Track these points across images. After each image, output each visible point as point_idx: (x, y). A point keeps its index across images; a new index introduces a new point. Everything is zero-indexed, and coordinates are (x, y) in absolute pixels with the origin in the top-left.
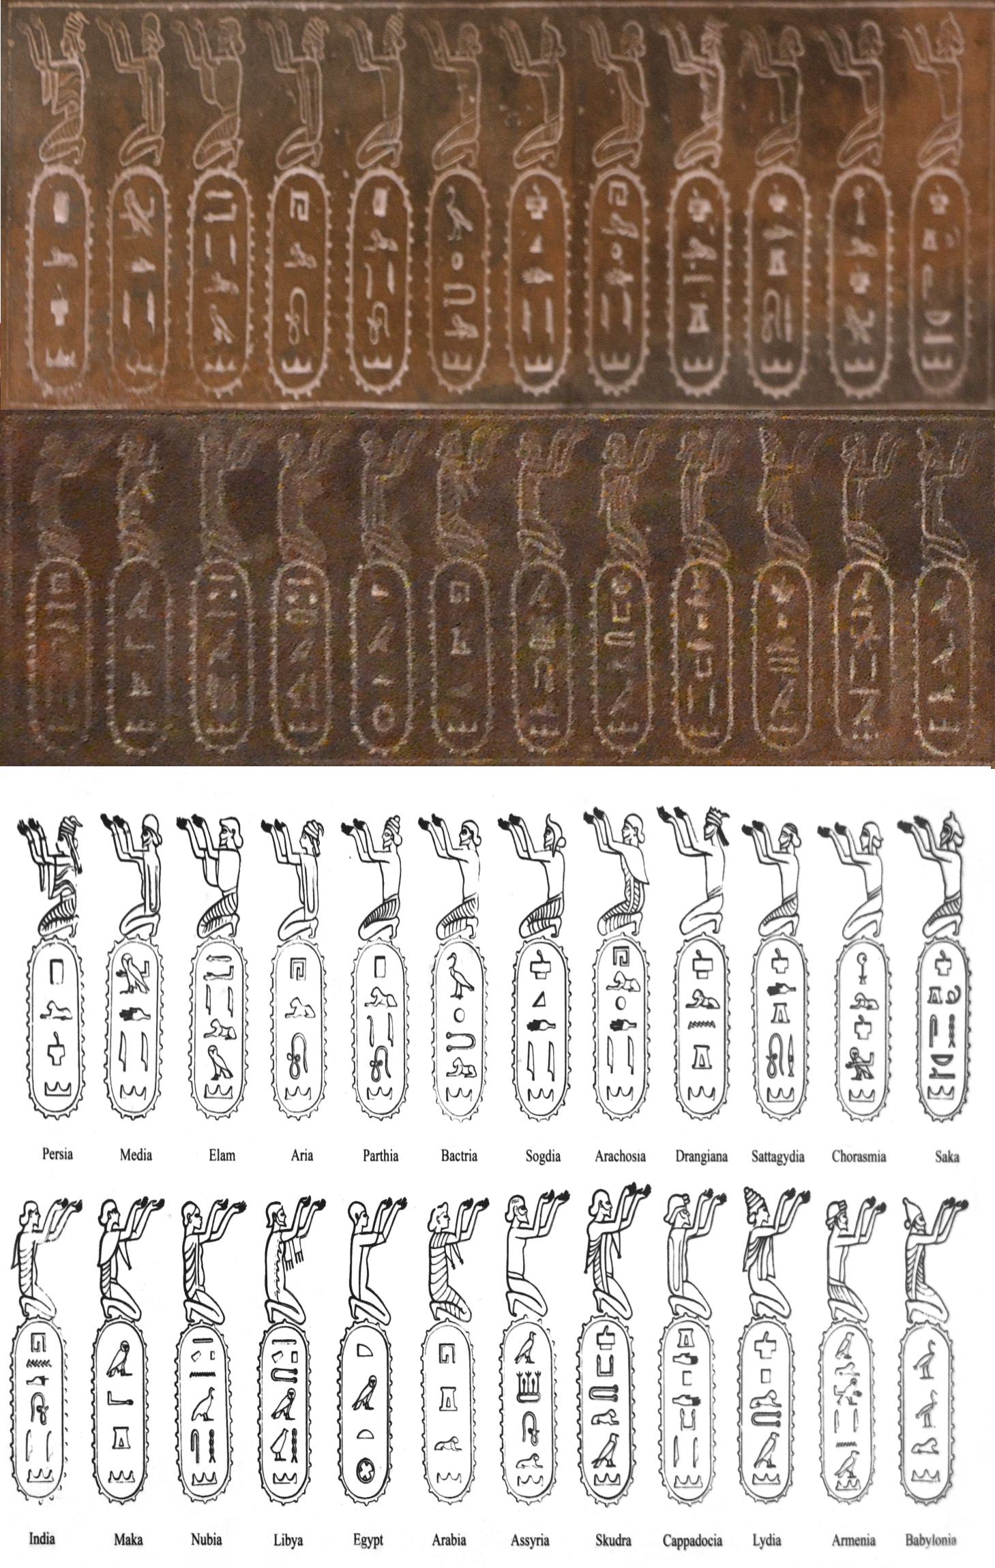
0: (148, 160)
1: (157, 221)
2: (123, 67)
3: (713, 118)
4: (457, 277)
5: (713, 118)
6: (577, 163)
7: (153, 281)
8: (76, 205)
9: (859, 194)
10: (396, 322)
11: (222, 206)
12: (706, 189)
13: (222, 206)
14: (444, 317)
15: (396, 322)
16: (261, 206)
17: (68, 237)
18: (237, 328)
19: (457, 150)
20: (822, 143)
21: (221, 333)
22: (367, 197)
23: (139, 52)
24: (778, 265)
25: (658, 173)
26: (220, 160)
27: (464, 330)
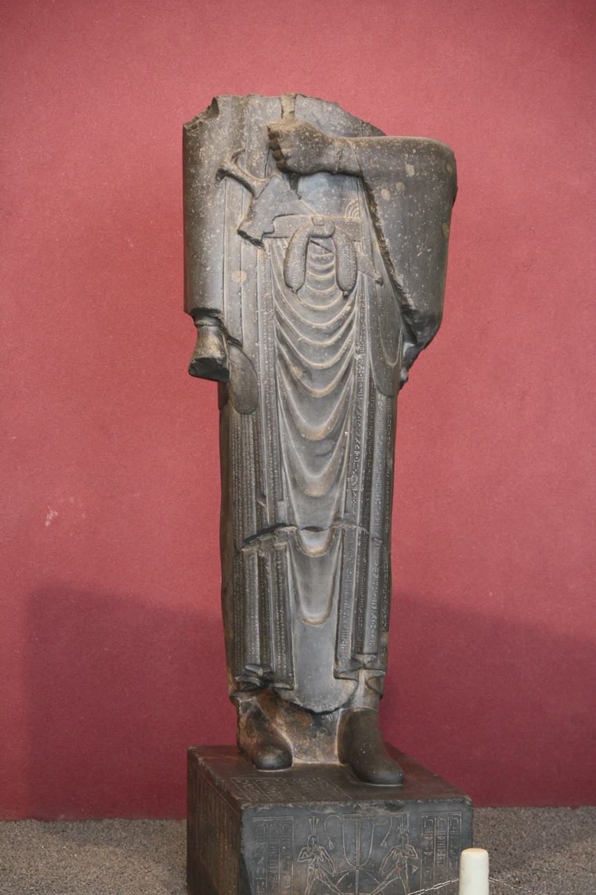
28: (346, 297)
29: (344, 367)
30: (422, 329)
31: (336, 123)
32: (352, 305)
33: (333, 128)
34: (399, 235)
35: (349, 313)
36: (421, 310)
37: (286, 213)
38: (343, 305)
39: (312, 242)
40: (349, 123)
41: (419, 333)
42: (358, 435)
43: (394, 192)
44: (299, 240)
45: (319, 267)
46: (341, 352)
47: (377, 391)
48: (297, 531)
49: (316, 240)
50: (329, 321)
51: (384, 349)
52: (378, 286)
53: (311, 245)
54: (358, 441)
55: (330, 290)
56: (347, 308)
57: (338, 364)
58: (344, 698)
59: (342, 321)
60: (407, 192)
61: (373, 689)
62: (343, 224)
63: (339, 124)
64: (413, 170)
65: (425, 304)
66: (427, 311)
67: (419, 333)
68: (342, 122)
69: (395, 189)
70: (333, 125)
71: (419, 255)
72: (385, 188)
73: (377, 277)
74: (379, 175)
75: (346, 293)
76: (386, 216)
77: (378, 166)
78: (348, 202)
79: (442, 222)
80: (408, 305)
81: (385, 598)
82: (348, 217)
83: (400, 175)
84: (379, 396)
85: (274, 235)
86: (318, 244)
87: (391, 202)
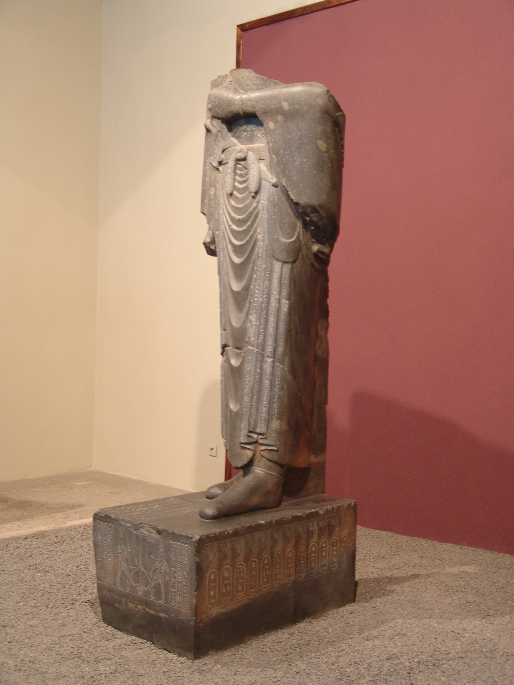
0: (228, 565)
1: (229, 574)
2: (224, 550)
3: (315, 536)
4: (278, 569)
5: (315, 536)
6: (296, 547)
7: (229, 584)
8: (215, 575)
9: (335, 541)
10: (268, 578)
11: (240, 568)
12: (314, 546)
13: (240, 568)
14: (276, 575)
15: (268, 578)
16: (247, 567)
17: (214, 581)
18: (243, 587)
19: (278, 549)
20: (330, 534)
21: (240, 588)
22: (264, 560)
23: (227, 547)
24: (324, 554)
25: (307, 545)
26: (240, 561)
27: (279, 576)
28: (253, 197)
29: (252, 243)
30: (308, 216)
31: (251, 83)
32: (258, 202)
33: (249, 87)
34: (282, 151)
35: (256, 207)
36: (301, 202)
37: (227, 147)
38: (251, 204)
39: (239, 164)
40: (258, 81)
41: (308, 219)
42: (257, 287)
43: (277, 122)
44: (231, 163)
45: (241, 179)
46: (251, 233)
47: (273, 259)
48: (231, 349)
49: (239, 163)
50: (245, 213)
51: (279, 230)
52: (274, 188)
53: (239, 166)
54: (257, 291)
55: (246, 194)
56: (255, 205)
57: (248, 242)
58: (245, 461)
59: (251, 213)
60: (285, 121)
61: (265, 458)
62: (254, 150)
63: (253, 83)
64: (287, 106)
65: (304, 198)
66: (307, 203)
67: (308, 219)
68: (254, 82)
69: (277, 121)
70: (248, 85)
71: (296, 164)
72: (270, 121)
73: (274, 180)
74: (266, 113)
75: (253, 194)
76: (273, 140)
77: (264, 106)
78: (257, 134)
79: (316, 139)
80: (292, 200)
81: (276, 397)
82: (256, 145)
83: (279, 111)
84: (275, 262)
85: (224, 162)
86: (241, 165)
87: (275, 130)
